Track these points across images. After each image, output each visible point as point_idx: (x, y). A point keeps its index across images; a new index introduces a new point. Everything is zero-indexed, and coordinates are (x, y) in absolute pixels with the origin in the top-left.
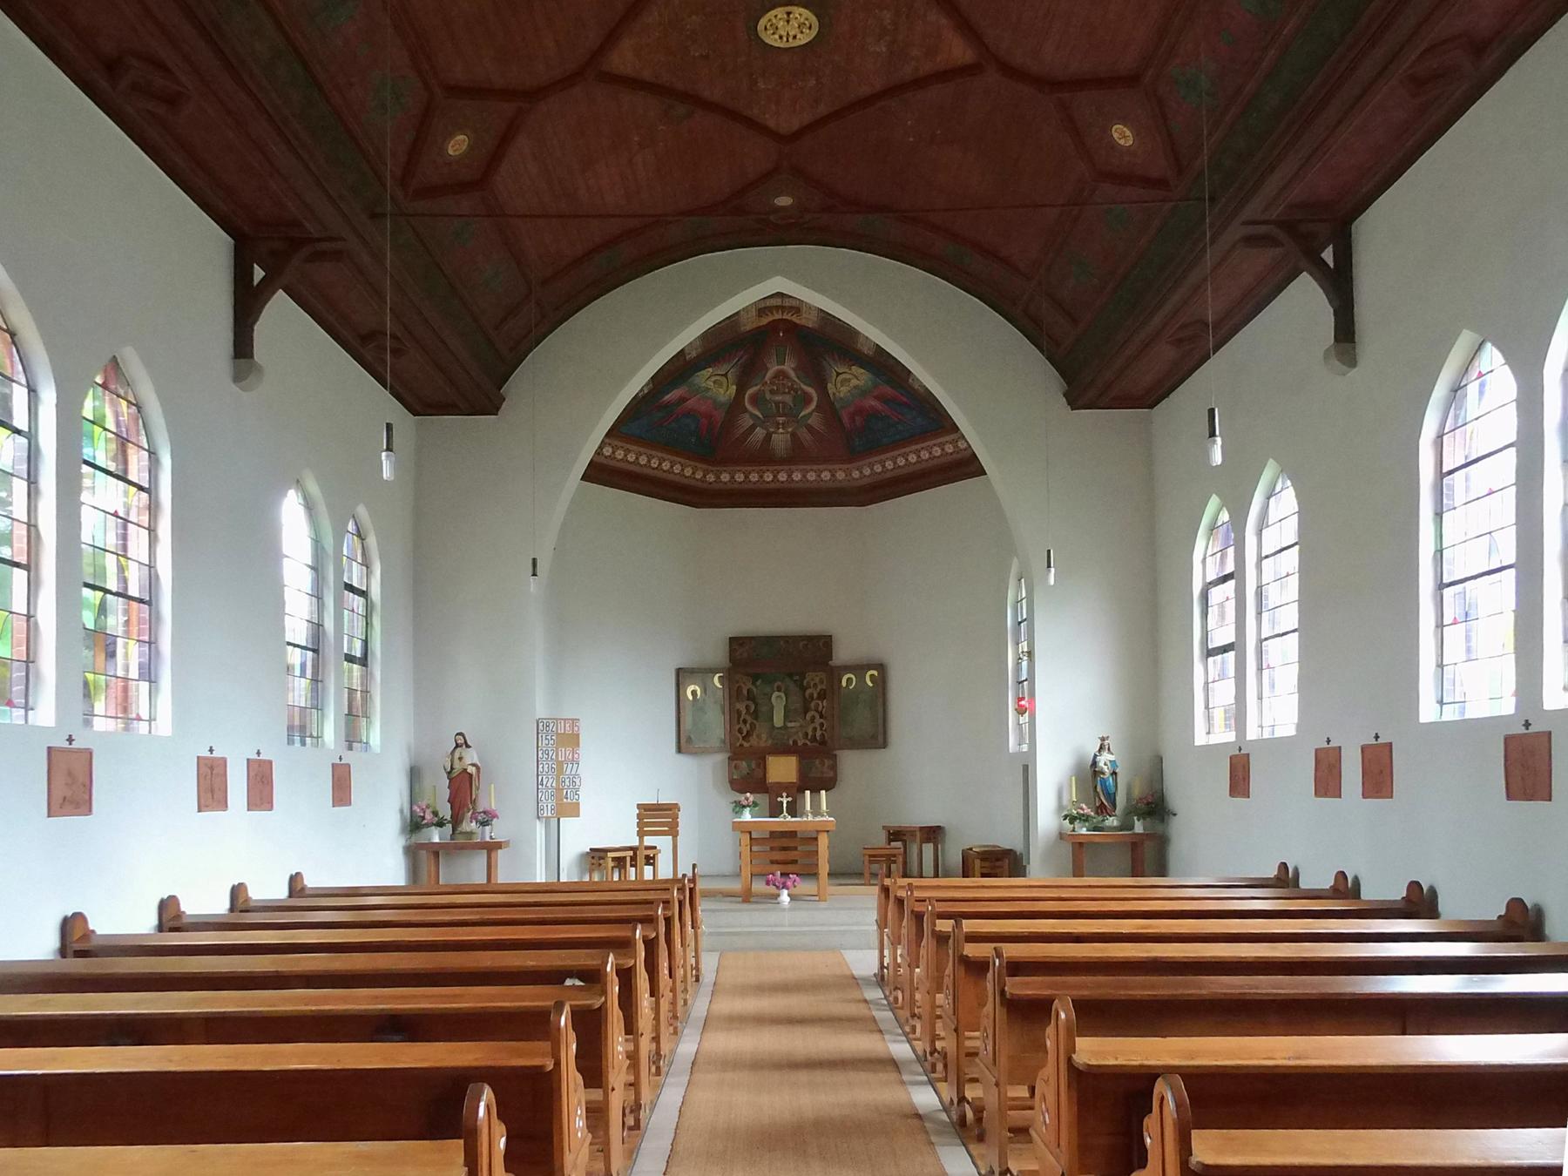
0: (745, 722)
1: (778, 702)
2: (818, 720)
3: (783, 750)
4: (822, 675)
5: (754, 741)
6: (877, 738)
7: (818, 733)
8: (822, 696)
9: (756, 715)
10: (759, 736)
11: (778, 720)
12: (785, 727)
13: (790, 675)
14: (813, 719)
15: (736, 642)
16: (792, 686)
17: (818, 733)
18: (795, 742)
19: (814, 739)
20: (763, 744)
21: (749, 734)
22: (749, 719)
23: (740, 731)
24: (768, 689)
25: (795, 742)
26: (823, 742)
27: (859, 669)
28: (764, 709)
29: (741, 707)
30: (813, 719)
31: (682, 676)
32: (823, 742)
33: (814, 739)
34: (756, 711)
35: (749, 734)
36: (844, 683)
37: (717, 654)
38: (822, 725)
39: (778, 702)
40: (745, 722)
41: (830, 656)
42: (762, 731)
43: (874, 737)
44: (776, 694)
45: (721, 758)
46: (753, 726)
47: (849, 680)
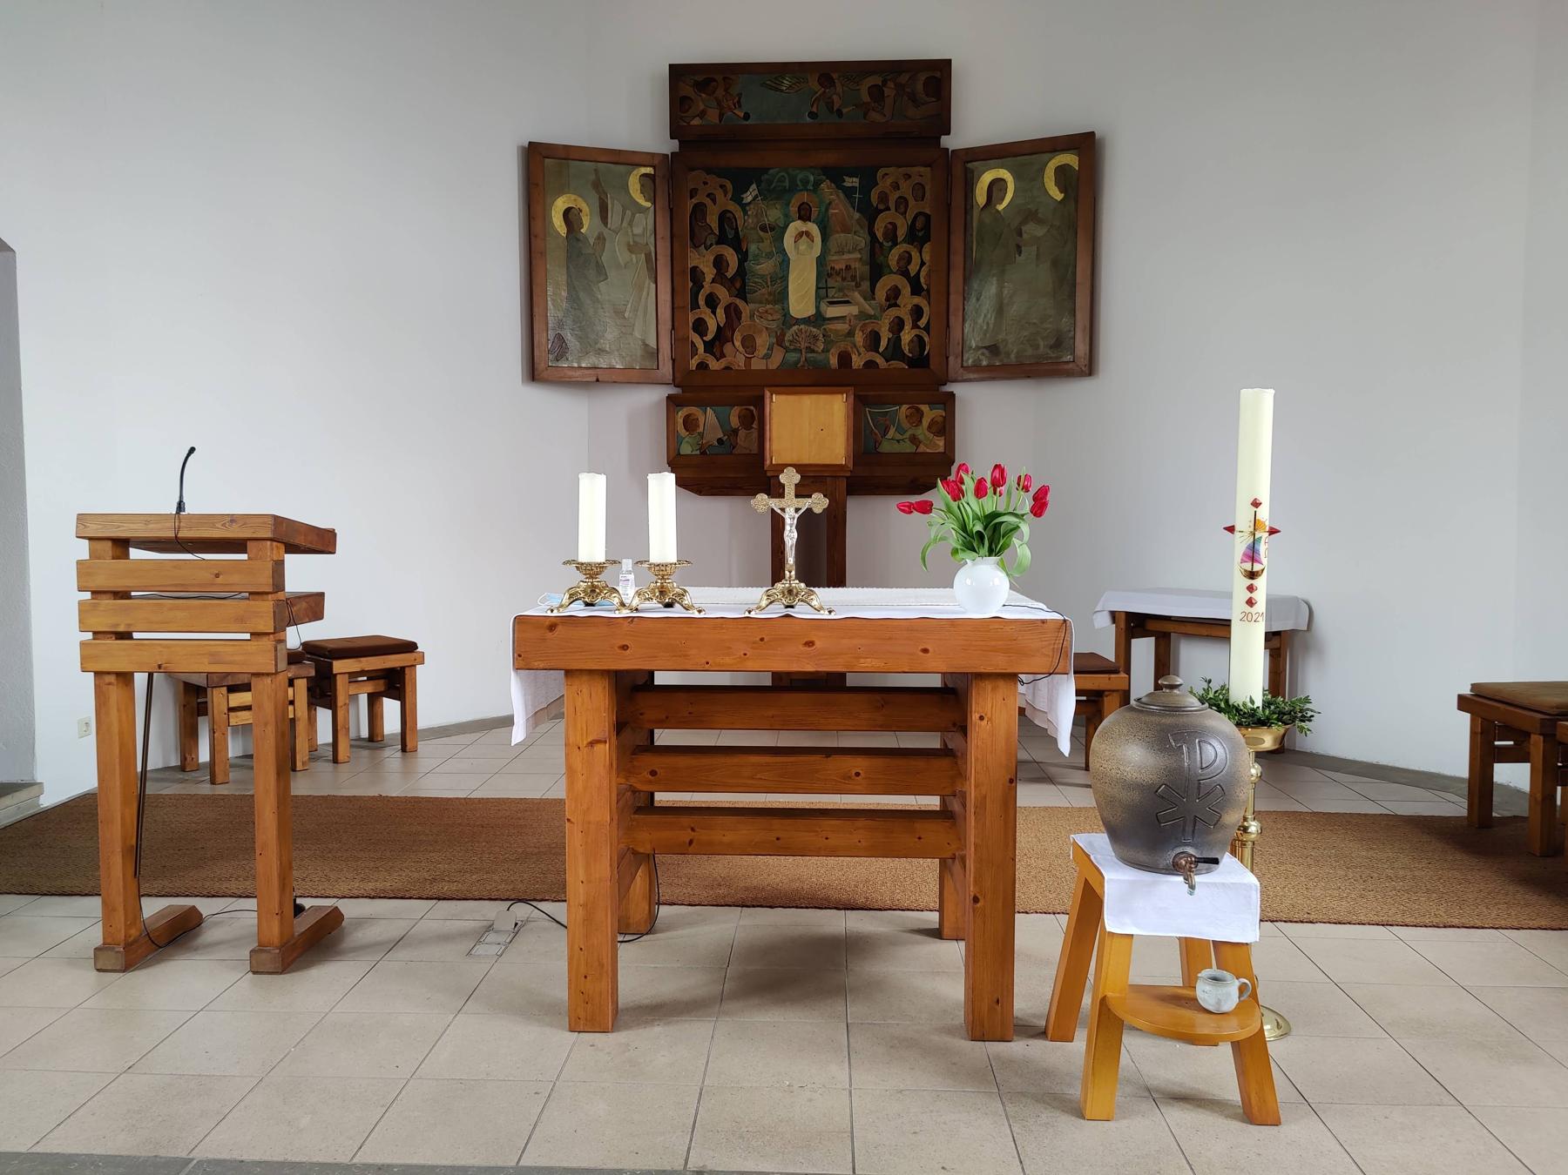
0: (712, 302)
1: (802, 253)
2: (908, 300)
3: (809, 378)
4: (922, 173)
5: (735, 355)
6: (1059, 349)
7: (907, 336)
8: (918, 236)
9: (740, 285)
10: (749, 344)
11: (801, 301)
12: (818, 319)
13: (835, 175)
14: (894, 294)
15: (692, 85)
16: (841, 208)
17: (907, 336)
18: (845, 359)
19: (895, 351)
20: (758, 364)
21: (723, 336)
22: (723, 294)
23: (700, 327)
24: (774, 215)
25: (845, 359)
26: (919, 361)
27: (1022, 154)
28: (765, 267)
29: (703, 261)
30: (894, 294)
31: (543, 166)
32: (919, 361)
33: (895, 351)
34: (742, 272)
35: (723, 336)
36: (981, 197)
37: (636, 122)
38: (917, 312)
39: (802, 253)
40: (712, 302)
41: (942, 122)
42: (756, 319)
43: (1060, 342)
44: (796, 226)
45: (652, 398)
46: (733, 313)
47: (997, 186)
